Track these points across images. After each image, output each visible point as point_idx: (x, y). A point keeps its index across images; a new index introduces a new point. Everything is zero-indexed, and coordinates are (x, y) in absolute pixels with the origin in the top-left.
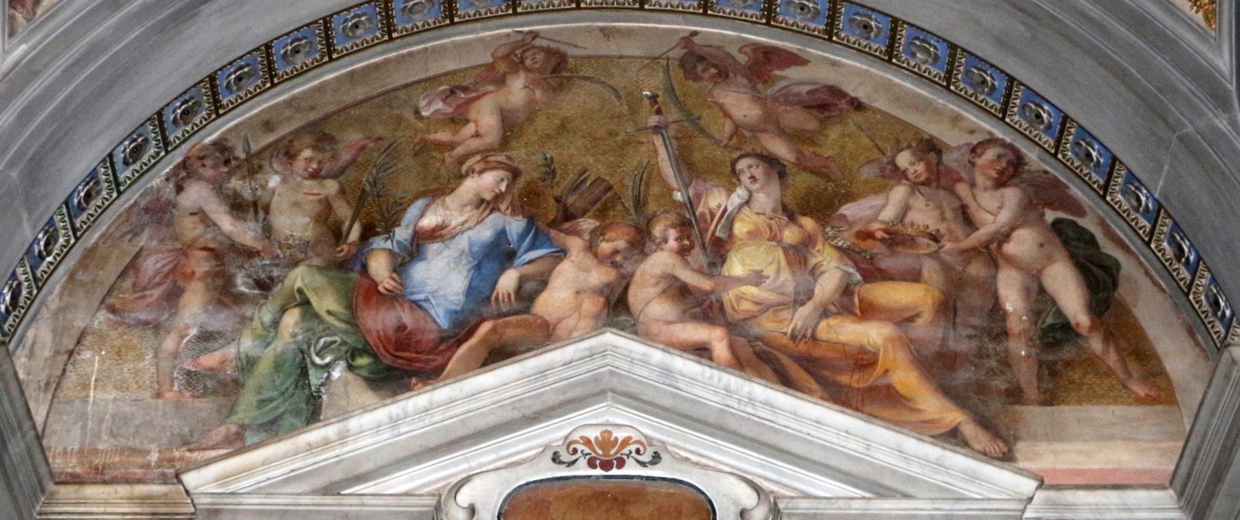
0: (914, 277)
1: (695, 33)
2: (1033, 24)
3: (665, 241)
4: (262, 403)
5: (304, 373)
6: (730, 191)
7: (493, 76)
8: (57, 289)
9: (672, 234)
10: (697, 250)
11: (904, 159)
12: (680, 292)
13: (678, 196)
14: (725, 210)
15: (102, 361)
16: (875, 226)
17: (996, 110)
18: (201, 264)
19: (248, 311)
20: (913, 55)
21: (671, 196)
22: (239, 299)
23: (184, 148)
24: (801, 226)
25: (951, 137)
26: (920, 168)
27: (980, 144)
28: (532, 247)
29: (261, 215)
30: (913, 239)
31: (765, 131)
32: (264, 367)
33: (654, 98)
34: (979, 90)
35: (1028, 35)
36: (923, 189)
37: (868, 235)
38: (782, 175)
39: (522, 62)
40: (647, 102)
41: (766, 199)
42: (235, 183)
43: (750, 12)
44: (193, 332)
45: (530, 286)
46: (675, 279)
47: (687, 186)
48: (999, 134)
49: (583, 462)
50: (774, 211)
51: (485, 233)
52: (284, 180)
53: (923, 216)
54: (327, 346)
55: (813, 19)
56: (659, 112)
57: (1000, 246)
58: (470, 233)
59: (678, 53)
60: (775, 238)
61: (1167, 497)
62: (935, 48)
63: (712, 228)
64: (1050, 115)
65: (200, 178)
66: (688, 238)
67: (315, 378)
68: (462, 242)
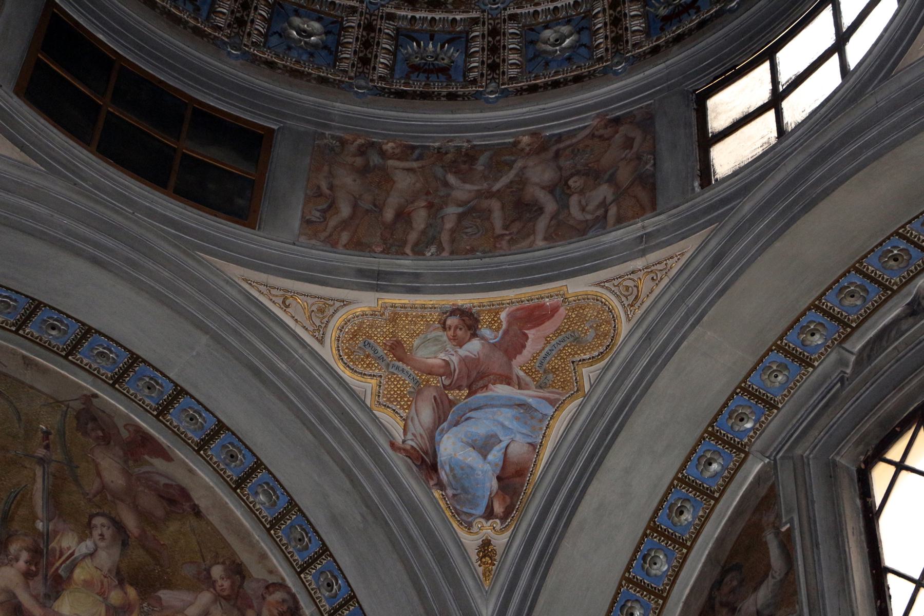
1: (95, 396)
3: (17, 560)
6: (81, 540)
9: (24, 556)
10: (39, 578)
11: (217, 571)
13: (40, 525)
14: (72, 554)
17: (297, 564)
20: (257, 494)
21: (34, 522)
24: (126, 593)
25: (255, 570)
26: (227, 584)
27: (273, 584)
31: (122, 501)
33: (47, 434)
34: (293, 544)
36: (223, 602)
38: (125, 544)
40: (40, 435)
41: (107, 558)
43: (148, 401)
46: (15, 596)
47: (50, 520)
50: (109, 571)
55: (194, 431)
56: (47, 447)
59: (77, 405)
62: (278, 498)
63: (57, 564)
64: (340, 588)
66: (36, 565)
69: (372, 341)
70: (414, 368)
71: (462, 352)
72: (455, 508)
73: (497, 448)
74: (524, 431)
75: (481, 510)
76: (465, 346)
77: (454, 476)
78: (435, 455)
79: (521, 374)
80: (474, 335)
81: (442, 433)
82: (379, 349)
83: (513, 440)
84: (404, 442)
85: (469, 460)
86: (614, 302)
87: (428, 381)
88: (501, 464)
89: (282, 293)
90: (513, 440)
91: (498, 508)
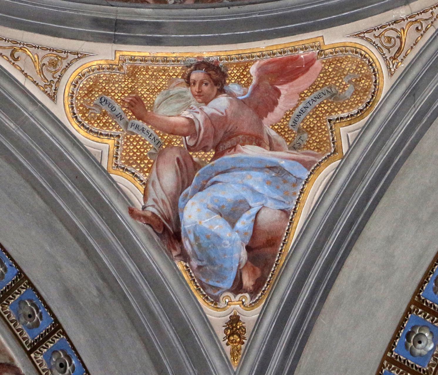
2: (107, 292)
17: (26, 343)
34: (22, 320)
35: (97, 300)
48: (18, 363)
62: (5, 269)
64: (73, 369)
69: (109, 98)
70: (155, 127)
71: (208, 109)
72: (200, 281)
73: (246, 215)
74: (276, 196)
75: (228, 283)
76: (212, 103)
77: (199, 246)
78: (178, 223)
79: (273, 133)
80: (221, 91)
81: (186, 199)
82: (117, 106)
83: (263, 206)
84: (144, 208)
85: (216, 229)
86: (375, 55)
87: (170, 142)
88: (250, 232)
89: (10, 44)
90: (263, 206)
91: (248, 281)
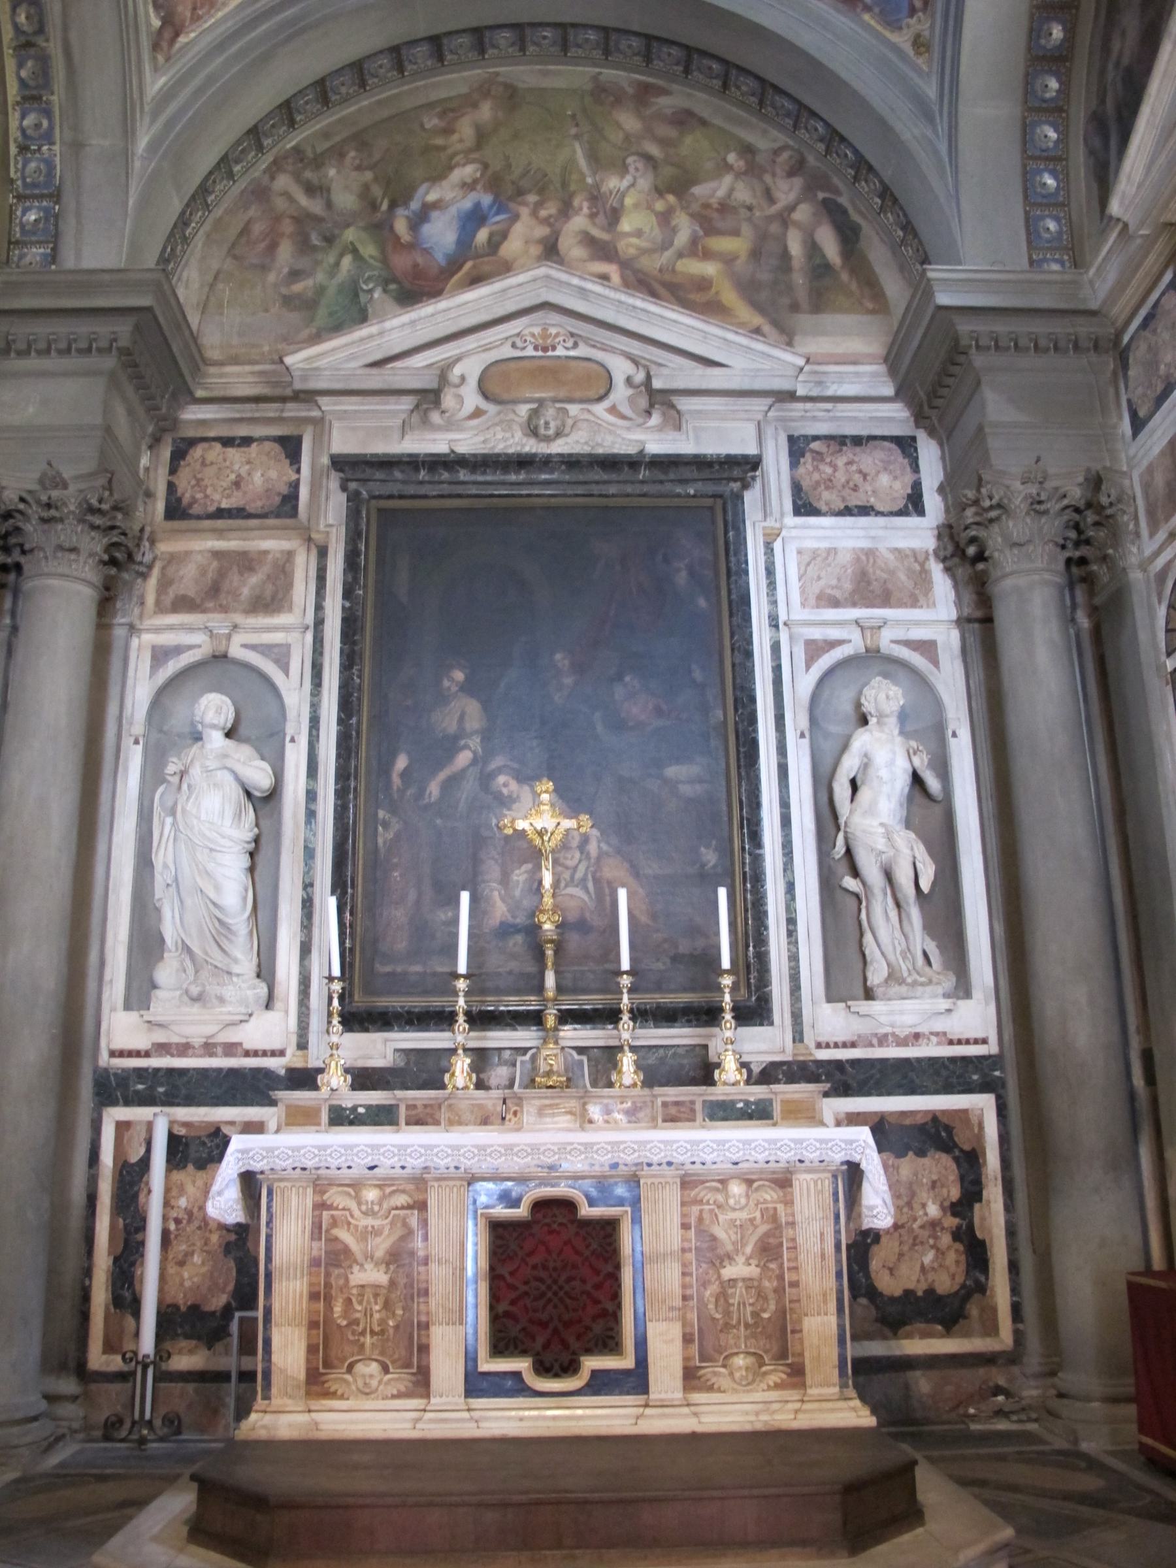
0: (736, 233)
1: (600, 73)
3: (581, 209)
4: (331, 314)
5: (356, 295)
6: (622, 177)
7: (470, 102)
8: (200, 245)
9: (585, 205)
11: (732, 158)
12: (589, 241)
15: (231, 289)
16: (713, 201)
18: (287, 227)
19: (320, 256)
22: (314, 249)
23: (275, 150)
28: (497, 213)
29: (325, 195)
30: (734, 208)
32: (332, 290)
33: (574, 116)
37: (707, 206)
38: (655, 168)
39: (489, 91)
41: (645, 183)
42: (308, 174)
44: (286, 270)
45: (496, 238)
48: (791, 143)
49: (531, 348)
51: (467, 204)
52: (338, 172)
53: (743, 194)
54: (370, 278)
56: (577, 125)
57: (789, 215)
58: (458, 205)
59: (589, 86)
60: (650, 207)
61: (882, 368)
65: (285, 171)
67: (363, 298)
68: (453, 210)
